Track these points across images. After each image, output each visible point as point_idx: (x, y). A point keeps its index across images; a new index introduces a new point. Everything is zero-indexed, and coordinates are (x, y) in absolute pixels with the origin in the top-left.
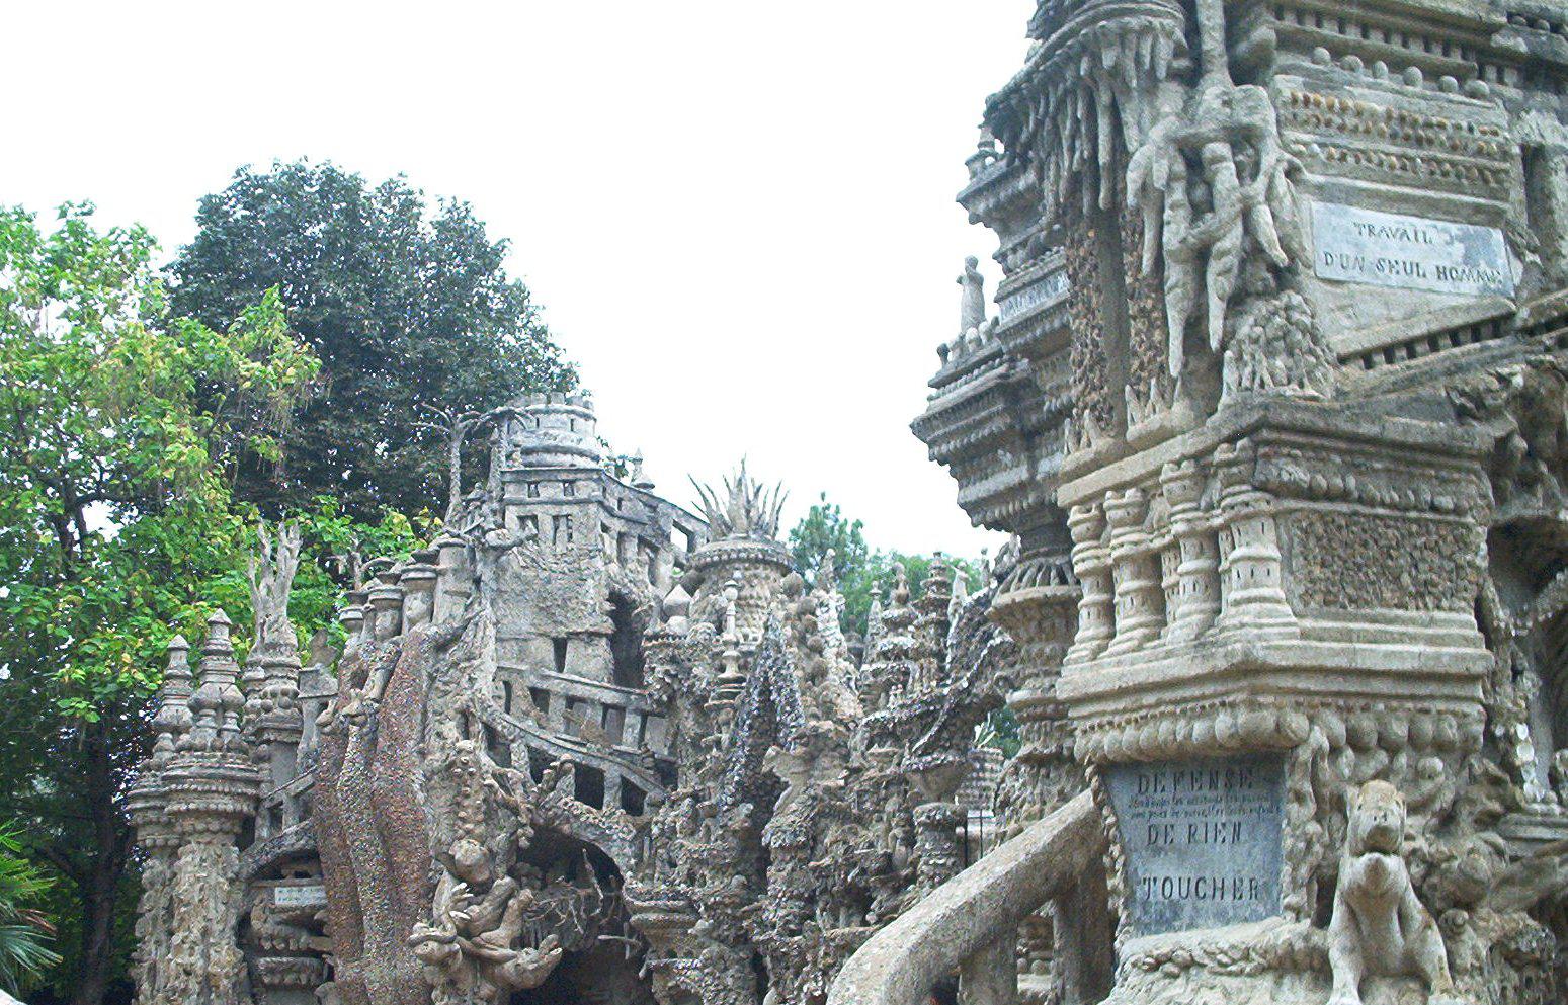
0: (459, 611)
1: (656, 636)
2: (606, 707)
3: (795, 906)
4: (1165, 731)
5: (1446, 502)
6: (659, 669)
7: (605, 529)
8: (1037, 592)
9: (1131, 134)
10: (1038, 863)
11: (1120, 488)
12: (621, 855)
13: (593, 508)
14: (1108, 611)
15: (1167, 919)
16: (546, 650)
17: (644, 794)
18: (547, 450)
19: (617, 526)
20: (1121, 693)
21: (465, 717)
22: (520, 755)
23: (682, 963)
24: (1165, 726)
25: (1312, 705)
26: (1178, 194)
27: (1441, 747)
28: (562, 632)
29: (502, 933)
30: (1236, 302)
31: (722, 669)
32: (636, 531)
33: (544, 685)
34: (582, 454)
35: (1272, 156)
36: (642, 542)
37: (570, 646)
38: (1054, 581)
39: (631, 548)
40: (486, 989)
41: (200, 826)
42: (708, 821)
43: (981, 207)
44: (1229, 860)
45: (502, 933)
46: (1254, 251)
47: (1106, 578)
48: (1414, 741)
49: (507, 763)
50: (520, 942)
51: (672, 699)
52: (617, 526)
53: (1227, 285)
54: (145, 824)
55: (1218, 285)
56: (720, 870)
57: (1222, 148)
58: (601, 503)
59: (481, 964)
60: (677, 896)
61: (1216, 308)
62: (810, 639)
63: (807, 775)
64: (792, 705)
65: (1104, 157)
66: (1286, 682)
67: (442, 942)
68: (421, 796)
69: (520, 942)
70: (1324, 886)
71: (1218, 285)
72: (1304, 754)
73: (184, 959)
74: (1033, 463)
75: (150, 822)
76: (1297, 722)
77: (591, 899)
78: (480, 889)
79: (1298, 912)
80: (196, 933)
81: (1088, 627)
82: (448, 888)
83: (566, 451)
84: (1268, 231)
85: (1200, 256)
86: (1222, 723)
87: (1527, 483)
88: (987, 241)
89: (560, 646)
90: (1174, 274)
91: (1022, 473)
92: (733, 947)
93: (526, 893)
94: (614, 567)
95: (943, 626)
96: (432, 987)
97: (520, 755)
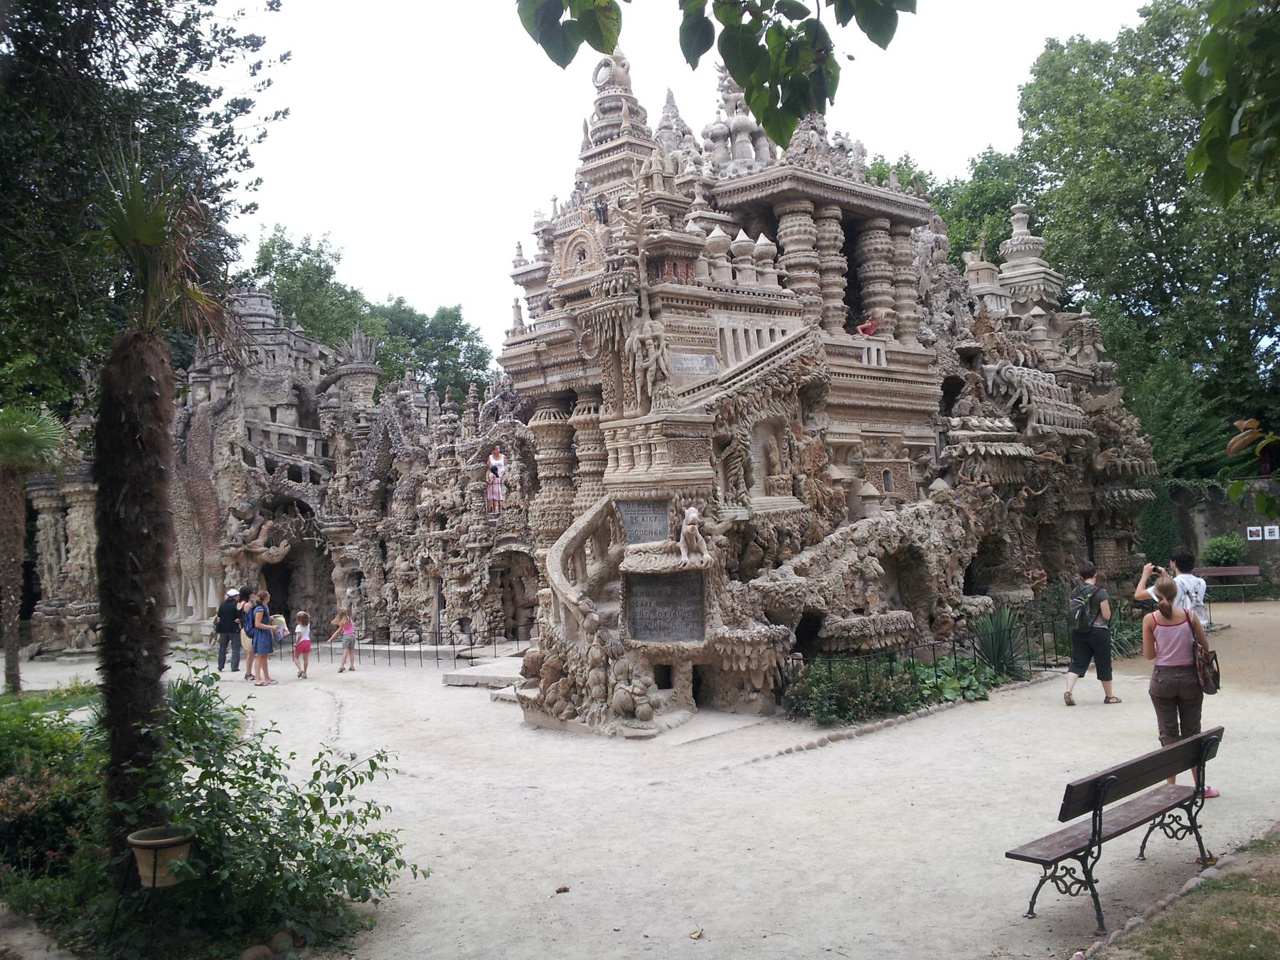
0: (224, 396)
1: (325, 408)
2: (298, 437)
3: (409, 523)
4: (636, 494)
5: (704, 435)
6: (328, 422)
7: (290, 356)
8: (546, 422)
9: (625, 333)
10: (590, 524)
11: (622, 428)
12: (313, 503)
13: (285, 347)
14: (617, 459)
15: (637, 540)
16: (266, 413)
17: (320, 476)
18: (251, 315)
19: (294, 354)
20: (623, 483)
21: (232, 446)
22: (260, 461)
23: (348, 547)
24: (636, 493)
25: (675, 488)
26: (640, 353)
27: (703, 496)
28: (274, 404)
29: (261, 540)
30: (654, 383)
31: (358, 421)
32: (302, 355)
33: (268, 429)
34: (267, 317)
35: (663, 343)
36: (306, 361)
37: (278, 411)
38: (553, 418)
39: (301, 362)
40: (254, 565)
41: (81, 499)
42: (358, 488)
43: (520, 280)
44: (656, 526)
45: (261, 540)
46: (659, 369)
47: (616, 451)
48: (697, 495)
49: (255, 465)
50: (267, 545)
51: (333, 435)
52: (294, 354)
53: (652, 379)
54: (38, 498)
55: (650, 378)
56: (366, 508)
57: (651, 341)
58: (288, 345)
59: (250, 555)
60: (345, 520)
61: (650, 384)
62: (406, 412)
63: (410, 469)
64: (400, 440)
65: (617, 338)
66: (670, 483)
67: (237, 547)
68: (213, 482)
69: (267, 545)
70: (678, 532)
71: (650, 378)
72: (674, 501)
73: (80, 561)
74: (545, 377)
75: (42, 497)
76: (672, 492)
77: (298, 524)
78: (250, 522)
79: (672, 539)
80: (84, 550)
81: (611, 464)
82: (233, 523)
83: (260, 316)
84: (663, 367)
85: (646, 370)
86: (653, 493)
87: (721, 426)
88: (521, 292)
89: (273, 411)
90: (638, 374)
91: (541, 382)
92: (371, 539)
93: (270, 523)
94: (295, 373)
95: (477, 414)
96: (225, 566)
97: (260, 461)
